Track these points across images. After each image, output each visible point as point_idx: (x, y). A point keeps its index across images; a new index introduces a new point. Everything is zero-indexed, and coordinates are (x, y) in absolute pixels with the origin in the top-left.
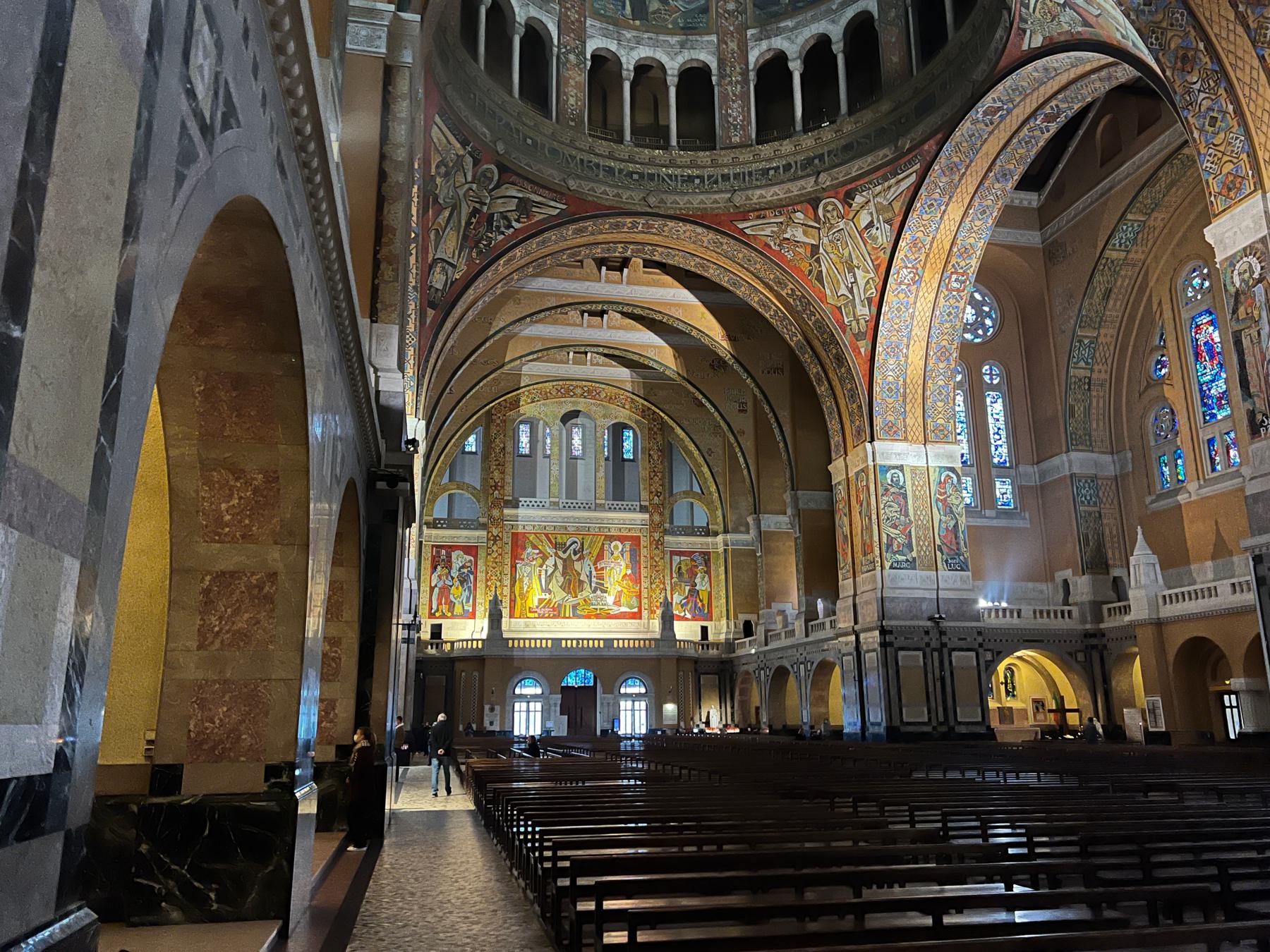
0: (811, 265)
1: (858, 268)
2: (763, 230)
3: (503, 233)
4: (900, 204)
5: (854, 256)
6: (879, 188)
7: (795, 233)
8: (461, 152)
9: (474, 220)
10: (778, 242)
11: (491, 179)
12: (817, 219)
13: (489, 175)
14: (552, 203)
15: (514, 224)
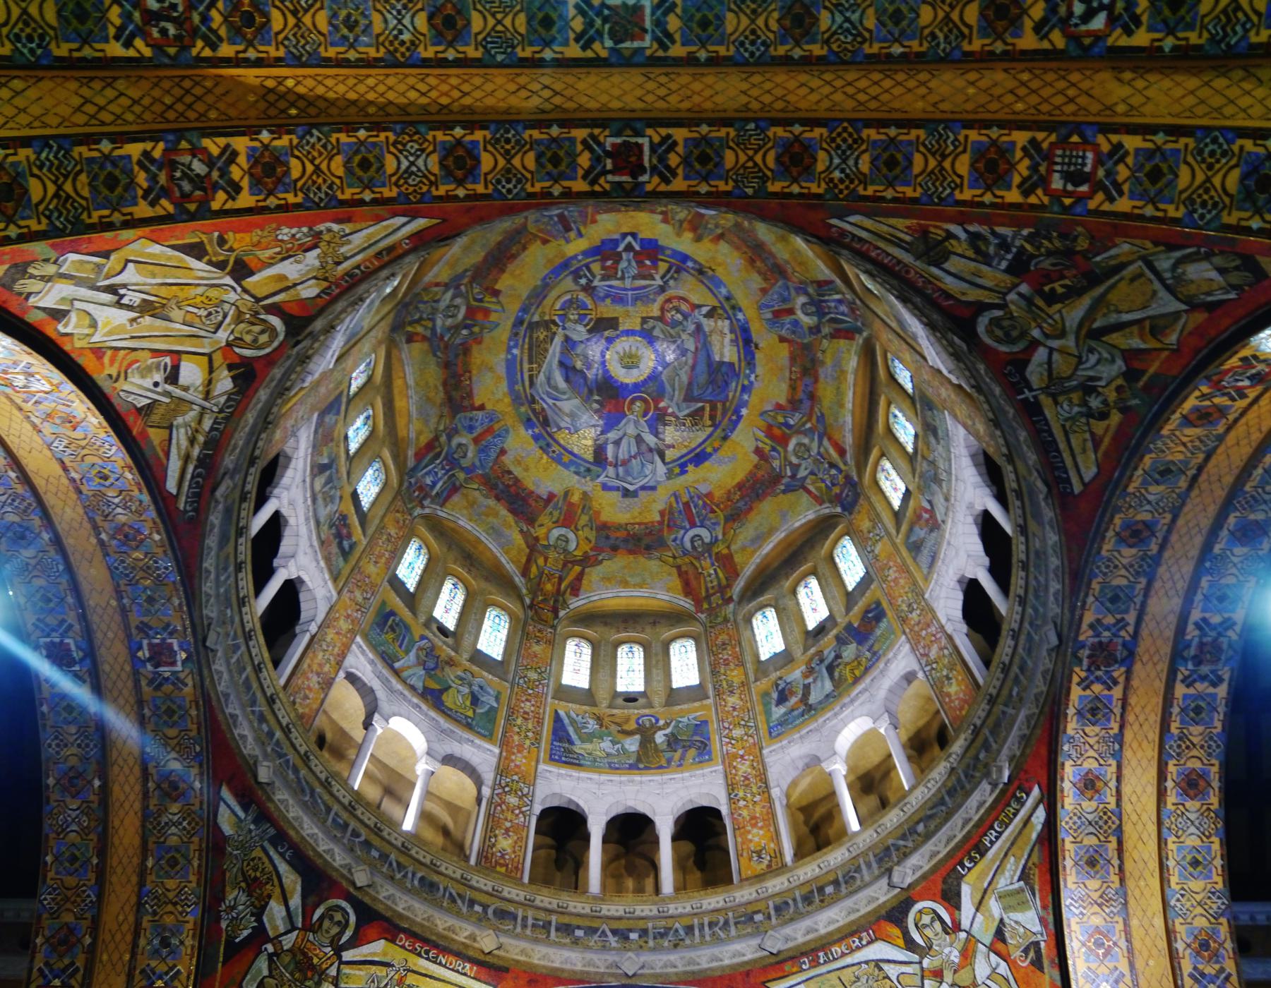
0: (231, 250)
1: (133, 320)
2: (369, 237)
3: (994, 233)
4: (156, 442)
5: (158, 322)
6: (207, 424)
7: (300, 267)
8: (1046, 401)
9: (1060, 290)
10: (326, 237)
11: (995, 322)
12: (275, 309)
13: (999, 333)
14: (864, 235)
15: (963, 236)
